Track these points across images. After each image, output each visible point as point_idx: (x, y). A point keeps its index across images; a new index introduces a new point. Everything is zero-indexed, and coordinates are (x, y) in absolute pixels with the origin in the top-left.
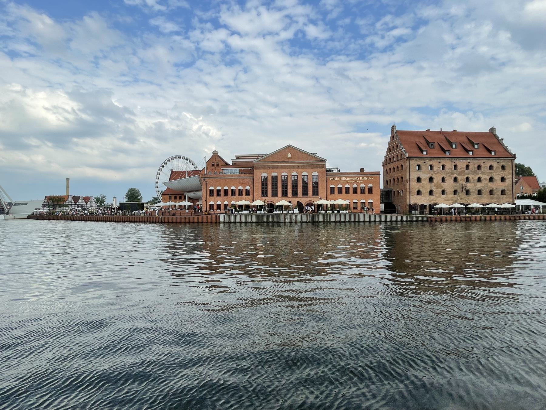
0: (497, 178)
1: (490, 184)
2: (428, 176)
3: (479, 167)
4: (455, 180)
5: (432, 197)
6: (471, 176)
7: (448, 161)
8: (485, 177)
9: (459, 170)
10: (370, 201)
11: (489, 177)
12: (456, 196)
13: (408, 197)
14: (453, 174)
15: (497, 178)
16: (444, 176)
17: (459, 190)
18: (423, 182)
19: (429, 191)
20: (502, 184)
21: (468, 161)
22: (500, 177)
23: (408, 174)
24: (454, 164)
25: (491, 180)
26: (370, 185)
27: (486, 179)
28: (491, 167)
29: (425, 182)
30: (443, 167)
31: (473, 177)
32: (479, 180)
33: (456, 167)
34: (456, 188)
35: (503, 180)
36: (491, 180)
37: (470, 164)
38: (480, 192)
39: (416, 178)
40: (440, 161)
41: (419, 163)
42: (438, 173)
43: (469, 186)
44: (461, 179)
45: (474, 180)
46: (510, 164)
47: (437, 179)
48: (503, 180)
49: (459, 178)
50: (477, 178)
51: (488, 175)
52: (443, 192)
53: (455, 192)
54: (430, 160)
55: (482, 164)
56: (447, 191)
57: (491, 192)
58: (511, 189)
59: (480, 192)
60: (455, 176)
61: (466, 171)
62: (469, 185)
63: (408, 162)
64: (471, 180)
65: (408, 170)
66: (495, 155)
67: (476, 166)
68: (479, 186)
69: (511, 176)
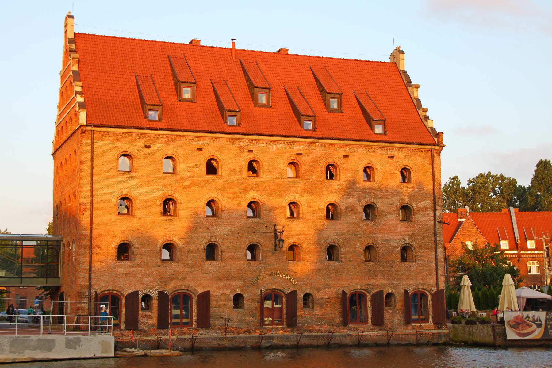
1: (367, 227)
2: (159, 193)
6: (303, 200)
7: (228, 145)
11: (364, 202)
14: (246, 190)
17: (266, 244)
20: (402, 226)
21: (297, 148)
23: (86, 186)
24: (250, 157)
27: (352, 209)
34: (254, 239)
41: (128, 147)
42: (194, 183)
45: (313, 213)
46: (427, 163)
50: (323, 205)
51: (359, 199)
52: (211, 251)
54: (167, 140)
56: (223, 247)
63: (87, 142)
64: (304, 209)
65: (86, 169)
66: (385, 133)
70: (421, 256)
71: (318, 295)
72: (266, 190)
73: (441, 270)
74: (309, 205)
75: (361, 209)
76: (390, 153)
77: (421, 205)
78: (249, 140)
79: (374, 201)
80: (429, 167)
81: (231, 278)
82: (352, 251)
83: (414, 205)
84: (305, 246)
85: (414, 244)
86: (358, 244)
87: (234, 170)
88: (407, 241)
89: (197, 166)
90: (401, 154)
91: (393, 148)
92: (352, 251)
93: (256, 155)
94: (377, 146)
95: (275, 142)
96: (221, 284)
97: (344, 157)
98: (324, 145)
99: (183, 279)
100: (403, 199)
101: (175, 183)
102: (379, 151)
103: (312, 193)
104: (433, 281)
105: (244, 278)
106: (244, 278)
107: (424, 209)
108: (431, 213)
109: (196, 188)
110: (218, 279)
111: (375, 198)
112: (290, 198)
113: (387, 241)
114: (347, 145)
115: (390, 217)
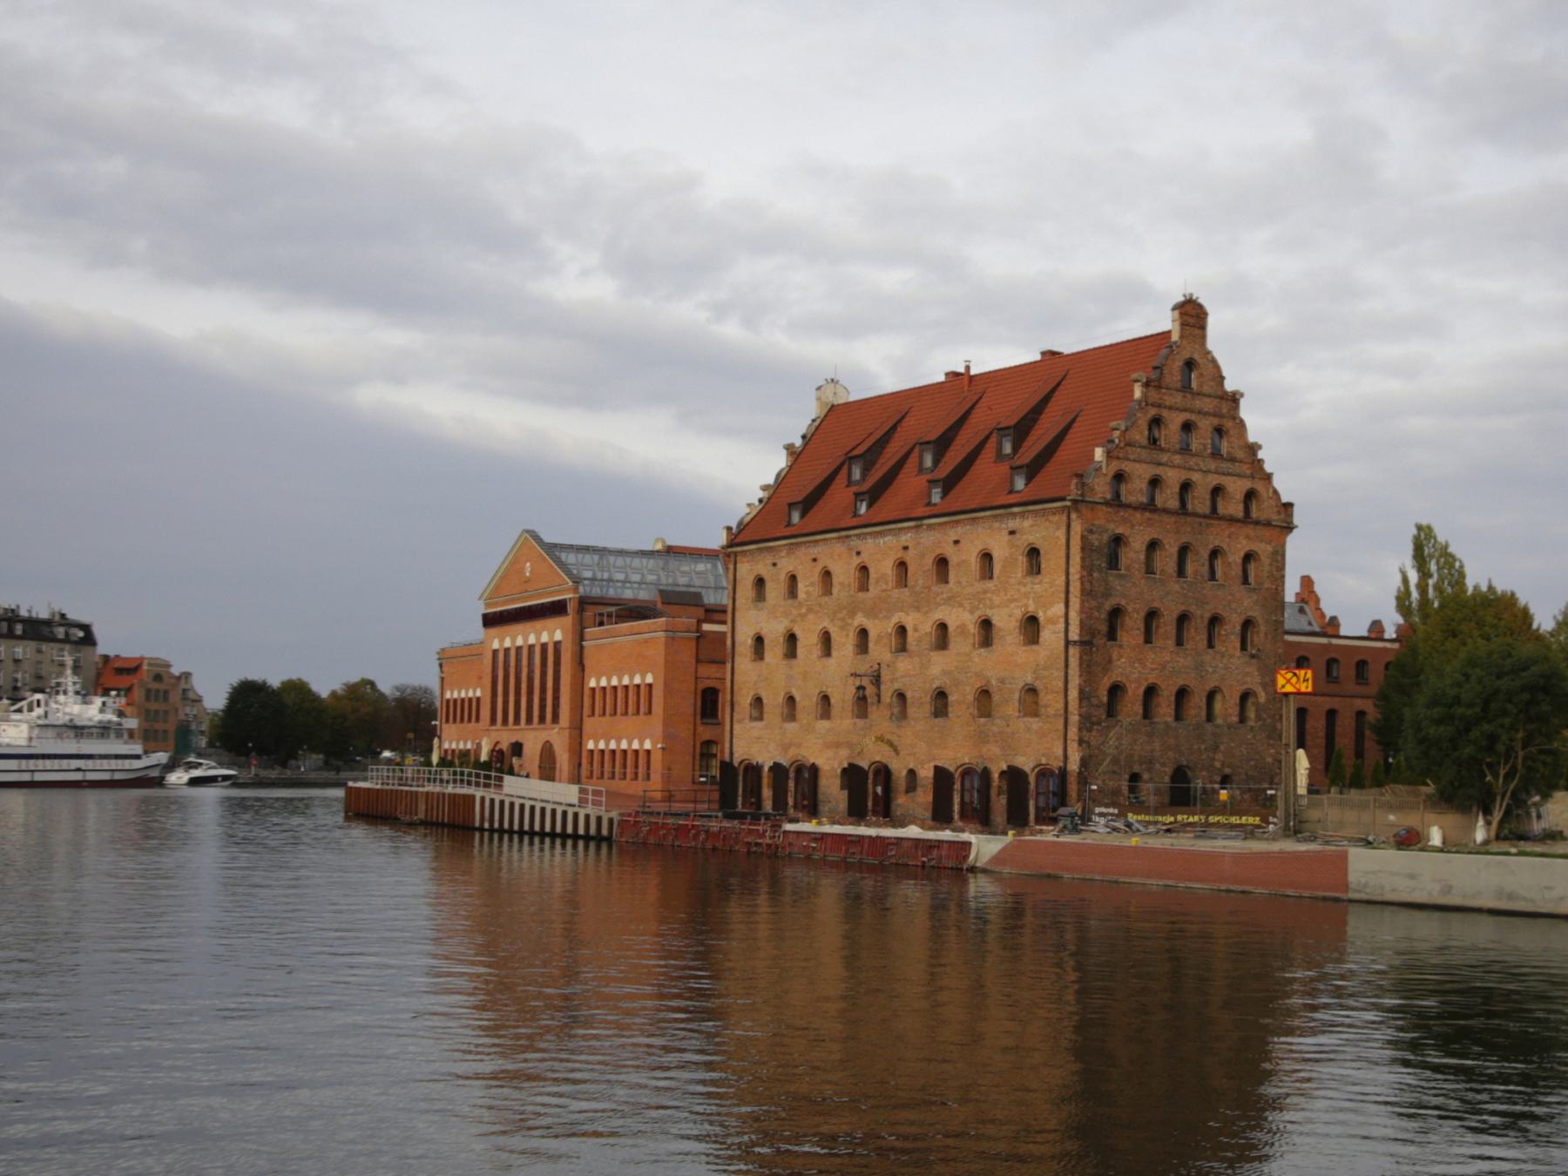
0: (1007, 621)
3: (942, 563)
5: (791, 726)
6: (909, 620)
7: (839, 548)
8: (961, 619)
9: (874, 590)
10: (648, 745)
13: (728, 728)
14: (852, 614)
15: (1007, 621)
16: (826, 624)
18: (768, 656)
19: (781, 699)
21: (906, 538)
22: (1018, 613)
26: (649, 679)
27: (962, 629)
28: (987, 557)
29: (774, 653)
31: (920, 625)
35: (1031, 626)
37: (909, 557)
39: (750, 642)
40: (815, 551)
42: (810, 610)
43: (905, 673)
44: (881, 629)
45: (919, 641)
46: (1061, 533)
47: (808, 642)
48: (1031, 626)
50: (928, 626)
51: (972, 613)
53: (862, 703)
55: (949, 551)
58: (1061, 684)
60: (860, 620)
61: (896, 593)
62: (904, 664)
67: (929, 561)
68: (939, 667)
69: (1059, 609)
70: (1046, 706)
72: (872, 612)
73: (1073, 732)
74: (916, 630)
75: (973, 629)
76: (1012, 524)
77: (1049, 613)
78: (858, 536)
79: (989, 613)
80: (1063, 541)
81: (838, 745)
82: (962, 698)
83: (1041, 615)
84: (909, 695)
85: (1039, 685)
86: (968, 689)
87: (841, 584)
88: (1029, 680)
89: (812, 584)
90: (1027, 523)
91: (1014, 515)
92: (962, 698)
93: (865, 558)
94: (995, 516)
95: (880, 534)
96: (830, 753)
97: (956, 542)
98: (930, 527)
99: (799, 745)
100: (1026, 606)
101: (795, 612)
102: (996, 525)
103: (918, 609)
104: (1060, 752)
105: (850, 745)
106: (850, 745)
107: (1052, 621)
108: (1061, 626)
109: (811, 617)
110: (828, 746)
111: (991, 607)
112: (895, 620)
113: (1002, 681)
114: (957, 522)
115: (1009, 639)
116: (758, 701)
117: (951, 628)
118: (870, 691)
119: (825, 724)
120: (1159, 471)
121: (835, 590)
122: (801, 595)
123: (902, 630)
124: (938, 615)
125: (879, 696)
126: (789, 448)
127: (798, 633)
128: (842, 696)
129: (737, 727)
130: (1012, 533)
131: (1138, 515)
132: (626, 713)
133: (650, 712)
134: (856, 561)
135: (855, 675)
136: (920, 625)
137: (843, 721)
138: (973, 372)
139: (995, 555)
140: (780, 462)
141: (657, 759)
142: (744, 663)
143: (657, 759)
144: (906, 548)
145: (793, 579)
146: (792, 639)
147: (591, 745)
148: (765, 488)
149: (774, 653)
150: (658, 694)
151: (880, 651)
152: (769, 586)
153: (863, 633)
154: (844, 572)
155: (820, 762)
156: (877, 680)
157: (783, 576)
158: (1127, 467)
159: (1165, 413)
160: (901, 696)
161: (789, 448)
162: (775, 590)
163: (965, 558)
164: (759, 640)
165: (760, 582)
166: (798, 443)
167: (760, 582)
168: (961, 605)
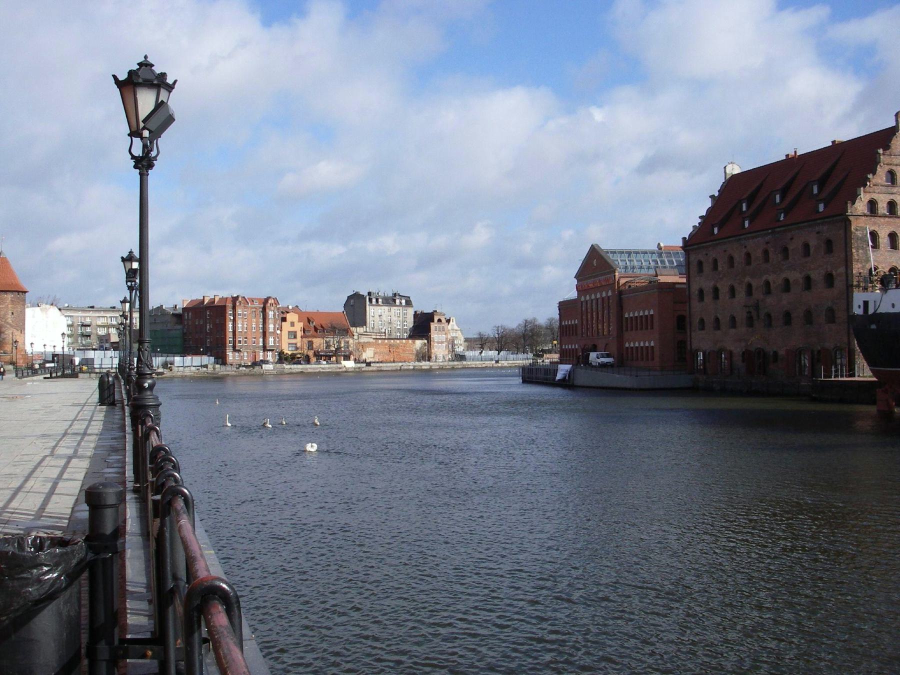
0: (817, 276)
2: (712, 284)
4: (749, 286)
5: (718, 332)
6: (771, 278)
8: (795, 276)
12: (750, 330)
15: (817, 276)
22: (823, 272)
25: (808, 282)
26: (652, 312)
28: (806, 246)
29: (708, 298)
30: (731, 259)
31: (776, 280)
32: (787, 286)
33: (748, 255)
35: (829, 279)
36: (808, 282)
38: (788, 318)
46: (842, 232)
47: (724, 290)
49: (754, 284)
50: (780, 281)
52: (733, 322)
53: (750, 322)
57: (808, 317)
59: (788, 318)
60: (748, 279)
62: (769, 300)
69: (842, 270)
71: (782, 352)
74: (774, 283)
76: (817, 229)
84: (772, 315)
90: (825, 228)
95: (756, 237)
108: (844, 278)
112: (764, 278)
116: (702, 321)
117: (791, 281)
118: (754, 314)
119: (734, 330)
120: (892, 197)
121: (736, 265)
122: (720, 269)
123: (767, 284)
124: (784, 275)
125: (758, 316)
126: (712, 197)
127: (719, 286)
128: (741, 316)
129: (693, 334)
130: (818, 233)
131: (882, 220)
132: (642, 329)
133: (652, 328)
134: (745, 250)
135: (745, 306)
136: (776, 280)
137: (742, 329)
138: (798, 154)
139: (811, 244)
140: (709, 204)
141: (657, 353)
142: (696, 305)
143: (657, 353)
144: (767, 243)
145: (715, 262)
146: (716, 290)
147: (627, 345)
148: (700, 217)
149: (708, 298)
150: (656, 320)
151: (758, 295)
152: (704, 265)
153: (749, 286)
154: (739, 257)
155: (732, 349)
156: (757, 307)
157: (710, 260)
158: (875, 196)
159: (894, 168)
160: (769, 316)
161: (712, 197)
162: (707, 268)
163: (795, 246)
164: (701, 291)
165: (700, 263)
166: (717, 194)
167: (700, 263)
168: (795, 270)
